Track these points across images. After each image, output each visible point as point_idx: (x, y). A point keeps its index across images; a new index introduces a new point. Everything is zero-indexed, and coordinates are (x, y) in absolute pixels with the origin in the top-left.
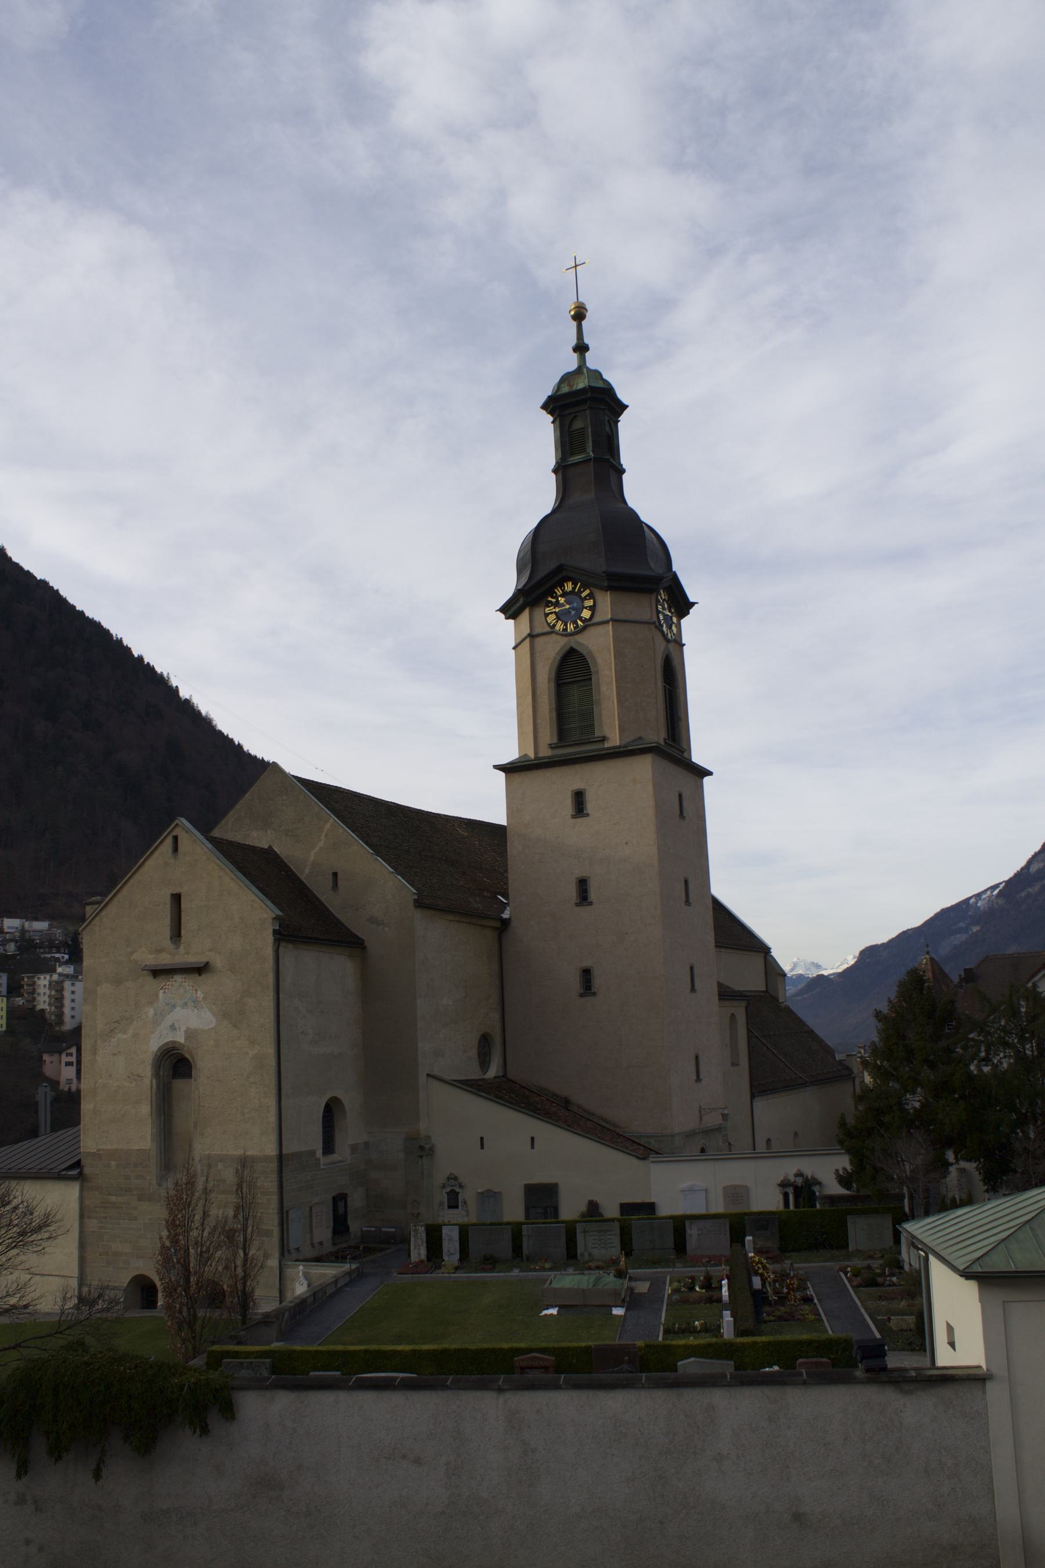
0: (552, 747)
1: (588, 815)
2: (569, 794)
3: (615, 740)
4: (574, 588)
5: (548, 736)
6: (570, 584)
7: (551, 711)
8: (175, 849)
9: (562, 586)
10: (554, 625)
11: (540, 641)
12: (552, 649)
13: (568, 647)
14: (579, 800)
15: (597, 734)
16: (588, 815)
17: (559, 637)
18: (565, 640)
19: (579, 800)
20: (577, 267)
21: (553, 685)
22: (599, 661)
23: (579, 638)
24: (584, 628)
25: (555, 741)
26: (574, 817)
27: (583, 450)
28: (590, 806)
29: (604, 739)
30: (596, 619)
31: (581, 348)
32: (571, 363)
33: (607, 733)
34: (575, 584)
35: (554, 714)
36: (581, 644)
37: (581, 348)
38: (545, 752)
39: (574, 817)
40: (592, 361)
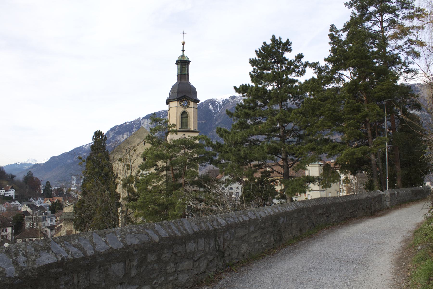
0: (180, 128)
3: (192, 129)
8: (144, 144)
11: (178, 108)
12: (181, 110)
18: (183, 109)
20: (185, 35)
23: (186, 109)
27: (184, 72)
29: (190, 129)
30: (190, 107)
31: (183, 51)
32: (181, 54)
33: (190, 128)
34: (186, 99)
37: (183, 51)
40: (186, 54)
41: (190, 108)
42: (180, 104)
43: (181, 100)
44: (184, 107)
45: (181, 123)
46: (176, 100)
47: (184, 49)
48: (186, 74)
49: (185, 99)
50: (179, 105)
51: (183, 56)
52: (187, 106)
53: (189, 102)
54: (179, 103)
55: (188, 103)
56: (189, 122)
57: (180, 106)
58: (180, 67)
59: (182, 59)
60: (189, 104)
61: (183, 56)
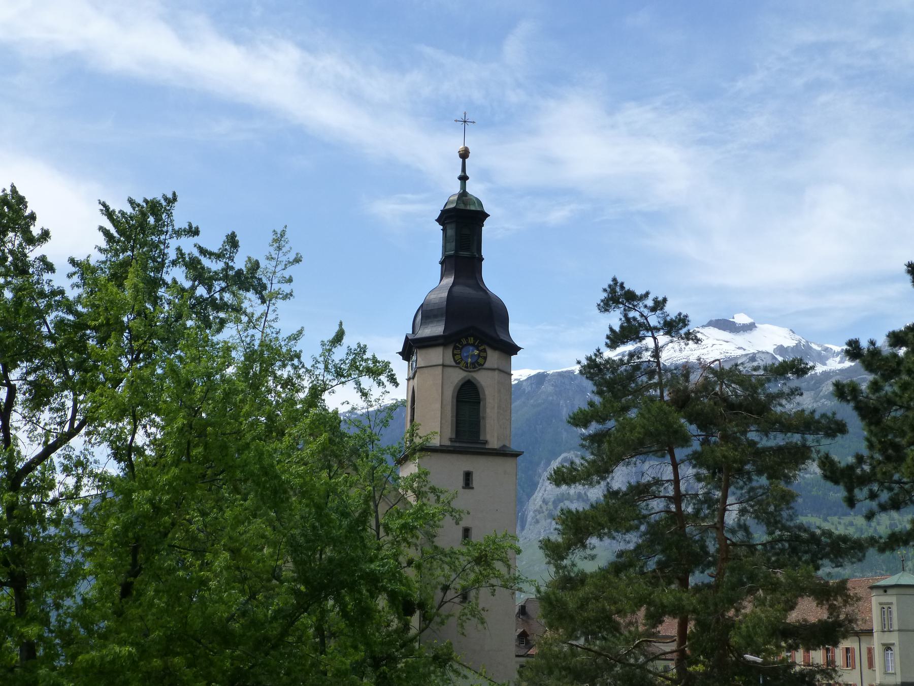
1: (472, 488)
2: (462, 473)
4: (474, 343)
5: (449, 432)
6: (472, 338)
7: (452, 417)
9: (466, 338)
10: (459, 363)
12: (457, 376)
13: (467, 379)
14: (468, 476)
15: (481, 438)
16: (472, 488)
17: (461, 371)
19: (468, 476)
21: (455, 401)
22: (487, 393)
24: (480, 369)
25: (454, 436)
26: (463, 488)
28: (476, 481)
29: (486, 442)
30: (487, 365)
31: (464, 178)
33: (488, 438)
34: (475, 339)
35: (455, 419)
36: (475, 379)
37: (464, 178)
38: (448, 443)
39: (463, 488)
40: (472, 188)
41: (490, 373)
42: (454, 355)
43: (460, 342)
44: (466, 368)
45: (457, 420)
46: (441, 341)
47: (468, 174)
48: (473, 257)
49: (471, 340)
50: (450, 361)
51: (463, 194)
52: (478, 365)
53: (485, 351)
54: (449, 352)
55: (483, 354)
56: (484, 418)
57: (453, 363)
58: (451, 232)
59: (462, 207)
60: (485, 358)
61: (463, 194)
